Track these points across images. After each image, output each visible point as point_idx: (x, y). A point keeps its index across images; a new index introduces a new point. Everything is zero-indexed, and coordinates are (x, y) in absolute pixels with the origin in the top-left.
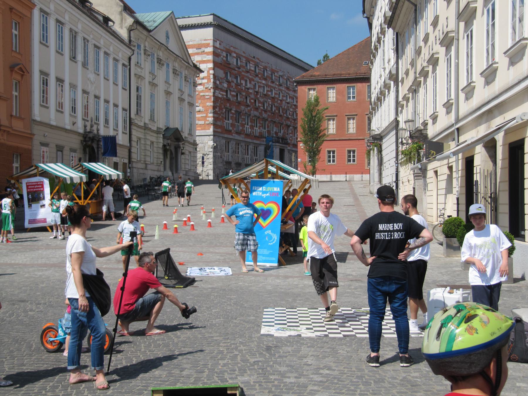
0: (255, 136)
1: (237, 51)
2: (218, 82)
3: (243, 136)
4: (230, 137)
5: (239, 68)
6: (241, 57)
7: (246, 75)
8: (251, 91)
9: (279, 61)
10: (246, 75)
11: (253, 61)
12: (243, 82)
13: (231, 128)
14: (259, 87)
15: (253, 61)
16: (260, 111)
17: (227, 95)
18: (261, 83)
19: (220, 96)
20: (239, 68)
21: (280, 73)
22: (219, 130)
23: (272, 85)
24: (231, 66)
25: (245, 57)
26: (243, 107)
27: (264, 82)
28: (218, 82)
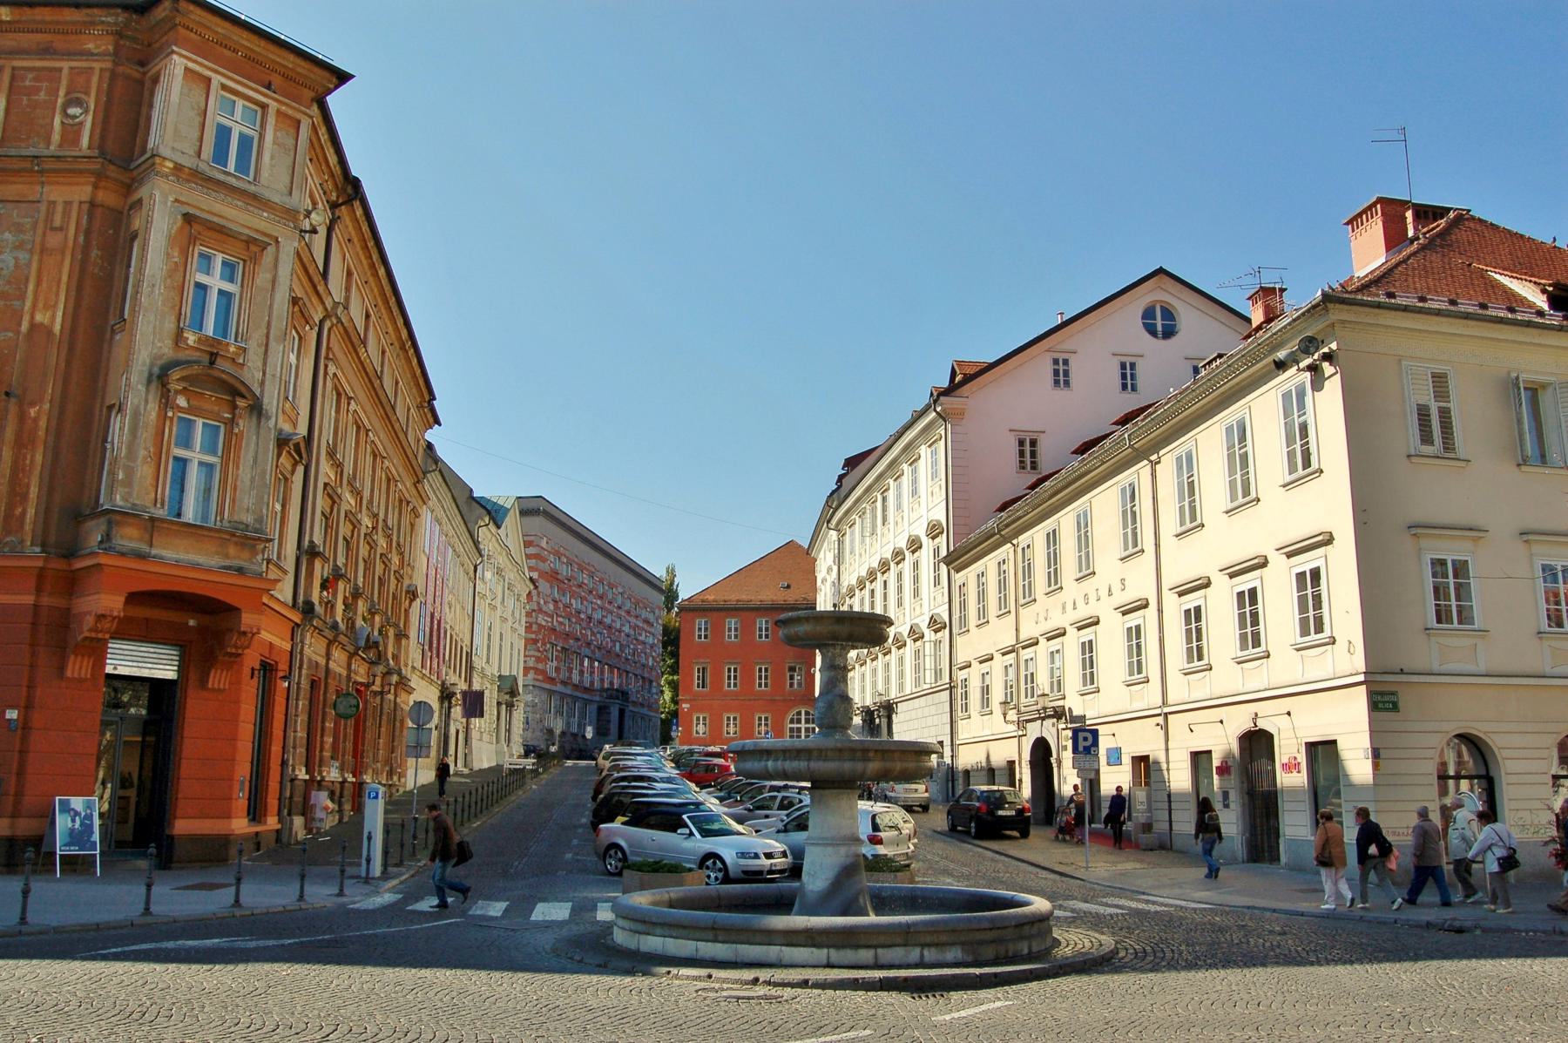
0: (585, 688)
1: (567, 553)
2: (542, 602)
3: (570, 687)
4: (554, 688)
5: (569, 580)
6: (574, 565)
7: (578, 590)
8: (583, 616)
9: (620, 570)
10: (578, 590)
11: (587, 570)
12: (573, 601)
13: (554, 675)
14: (593, 609)
15: (587, 570)
16: (592, 647)
17: (552, 622)
18: (596, 603)
19: (544, 623)
20: (569, 580)
21: (620, 590)
22: (540, 677)
23: (609, 607)
24: (559, 577)
25: (577, 564)
26: (571, 641)
27: (599, 602)
28: (542, 602)
